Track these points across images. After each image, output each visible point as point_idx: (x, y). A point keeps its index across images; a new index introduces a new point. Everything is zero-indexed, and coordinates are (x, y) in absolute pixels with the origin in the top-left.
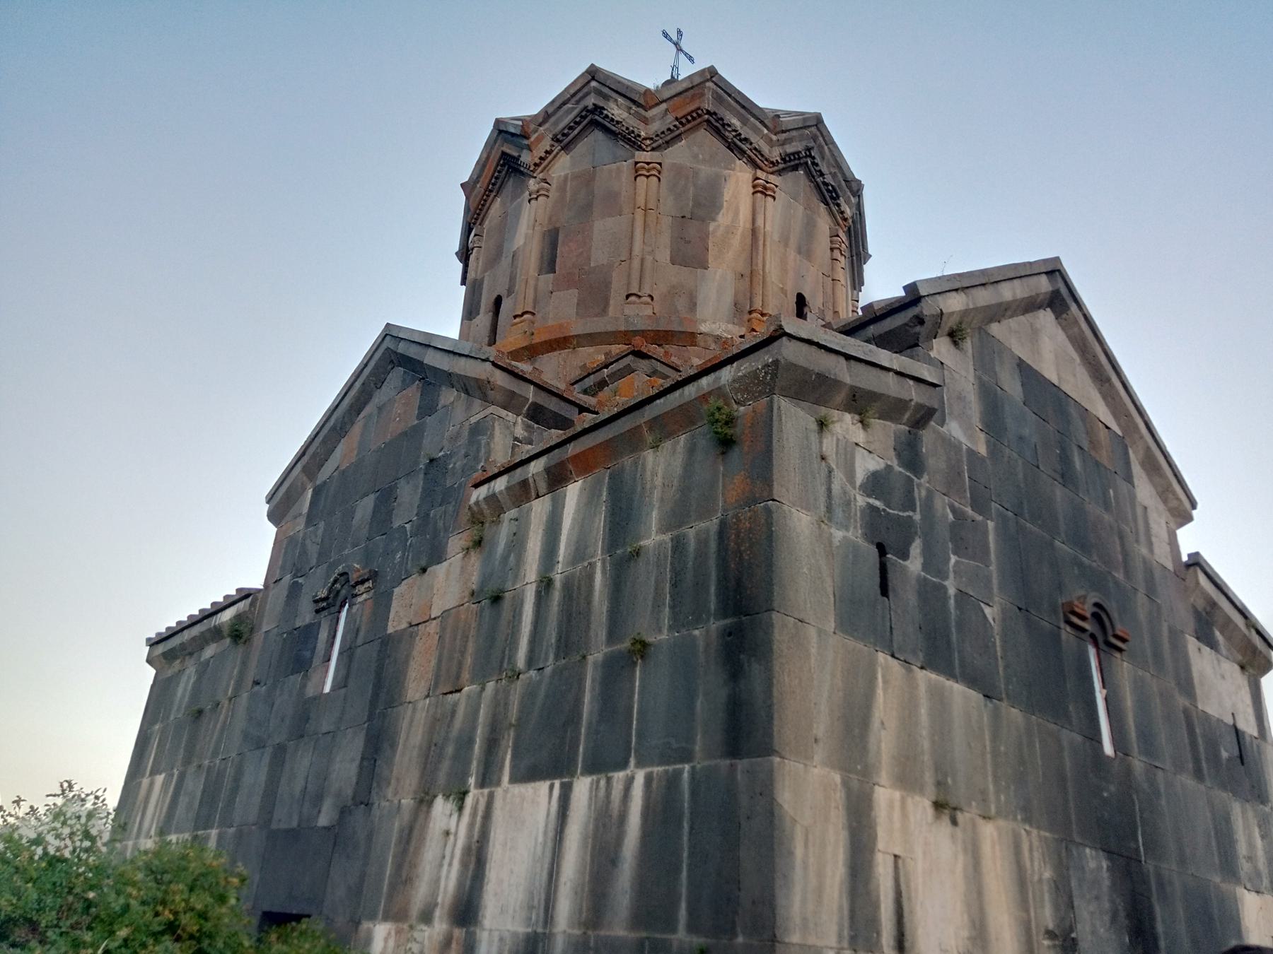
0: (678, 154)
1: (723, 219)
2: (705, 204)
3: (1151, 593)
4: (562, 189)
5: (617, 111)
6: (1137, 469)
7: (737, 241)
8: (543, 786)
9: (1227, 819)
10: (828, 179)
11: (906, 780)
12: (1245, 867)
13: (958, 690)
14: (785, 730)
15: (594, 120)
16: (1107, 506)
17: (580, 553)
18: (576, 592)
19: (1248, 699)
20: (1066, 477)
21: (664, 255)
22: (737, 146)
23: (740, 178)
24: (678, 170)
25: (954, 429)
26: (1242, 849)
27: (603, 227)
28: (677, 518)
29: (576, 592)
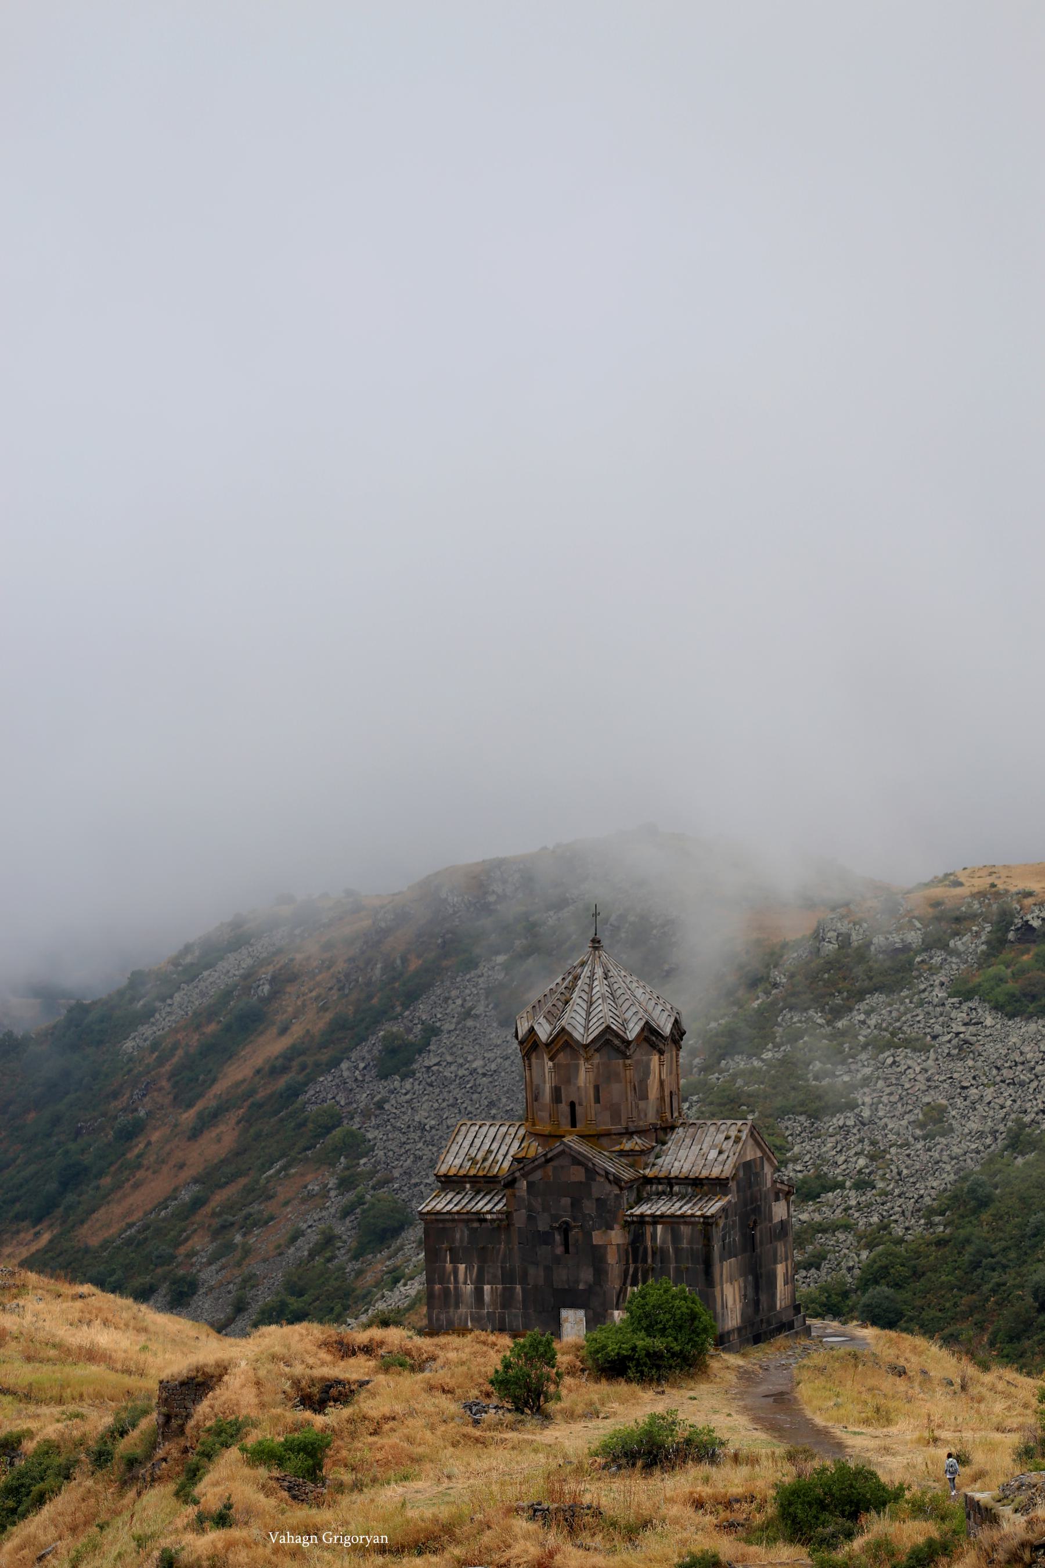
0: (637, 1056)
1: (651, 1077)
2: (647, 1073)
3: (765, 1198)
4: (598, 1067)
5: (616, 1042)
6: (765, 1162)
12: (779, 1258)
15: (608, 1042)
17: (664, 1241)
20: (750, 1187)
22: (653, 1046)
23: (655, 1058)
27: (616, 1088)
28: (690, 1242)
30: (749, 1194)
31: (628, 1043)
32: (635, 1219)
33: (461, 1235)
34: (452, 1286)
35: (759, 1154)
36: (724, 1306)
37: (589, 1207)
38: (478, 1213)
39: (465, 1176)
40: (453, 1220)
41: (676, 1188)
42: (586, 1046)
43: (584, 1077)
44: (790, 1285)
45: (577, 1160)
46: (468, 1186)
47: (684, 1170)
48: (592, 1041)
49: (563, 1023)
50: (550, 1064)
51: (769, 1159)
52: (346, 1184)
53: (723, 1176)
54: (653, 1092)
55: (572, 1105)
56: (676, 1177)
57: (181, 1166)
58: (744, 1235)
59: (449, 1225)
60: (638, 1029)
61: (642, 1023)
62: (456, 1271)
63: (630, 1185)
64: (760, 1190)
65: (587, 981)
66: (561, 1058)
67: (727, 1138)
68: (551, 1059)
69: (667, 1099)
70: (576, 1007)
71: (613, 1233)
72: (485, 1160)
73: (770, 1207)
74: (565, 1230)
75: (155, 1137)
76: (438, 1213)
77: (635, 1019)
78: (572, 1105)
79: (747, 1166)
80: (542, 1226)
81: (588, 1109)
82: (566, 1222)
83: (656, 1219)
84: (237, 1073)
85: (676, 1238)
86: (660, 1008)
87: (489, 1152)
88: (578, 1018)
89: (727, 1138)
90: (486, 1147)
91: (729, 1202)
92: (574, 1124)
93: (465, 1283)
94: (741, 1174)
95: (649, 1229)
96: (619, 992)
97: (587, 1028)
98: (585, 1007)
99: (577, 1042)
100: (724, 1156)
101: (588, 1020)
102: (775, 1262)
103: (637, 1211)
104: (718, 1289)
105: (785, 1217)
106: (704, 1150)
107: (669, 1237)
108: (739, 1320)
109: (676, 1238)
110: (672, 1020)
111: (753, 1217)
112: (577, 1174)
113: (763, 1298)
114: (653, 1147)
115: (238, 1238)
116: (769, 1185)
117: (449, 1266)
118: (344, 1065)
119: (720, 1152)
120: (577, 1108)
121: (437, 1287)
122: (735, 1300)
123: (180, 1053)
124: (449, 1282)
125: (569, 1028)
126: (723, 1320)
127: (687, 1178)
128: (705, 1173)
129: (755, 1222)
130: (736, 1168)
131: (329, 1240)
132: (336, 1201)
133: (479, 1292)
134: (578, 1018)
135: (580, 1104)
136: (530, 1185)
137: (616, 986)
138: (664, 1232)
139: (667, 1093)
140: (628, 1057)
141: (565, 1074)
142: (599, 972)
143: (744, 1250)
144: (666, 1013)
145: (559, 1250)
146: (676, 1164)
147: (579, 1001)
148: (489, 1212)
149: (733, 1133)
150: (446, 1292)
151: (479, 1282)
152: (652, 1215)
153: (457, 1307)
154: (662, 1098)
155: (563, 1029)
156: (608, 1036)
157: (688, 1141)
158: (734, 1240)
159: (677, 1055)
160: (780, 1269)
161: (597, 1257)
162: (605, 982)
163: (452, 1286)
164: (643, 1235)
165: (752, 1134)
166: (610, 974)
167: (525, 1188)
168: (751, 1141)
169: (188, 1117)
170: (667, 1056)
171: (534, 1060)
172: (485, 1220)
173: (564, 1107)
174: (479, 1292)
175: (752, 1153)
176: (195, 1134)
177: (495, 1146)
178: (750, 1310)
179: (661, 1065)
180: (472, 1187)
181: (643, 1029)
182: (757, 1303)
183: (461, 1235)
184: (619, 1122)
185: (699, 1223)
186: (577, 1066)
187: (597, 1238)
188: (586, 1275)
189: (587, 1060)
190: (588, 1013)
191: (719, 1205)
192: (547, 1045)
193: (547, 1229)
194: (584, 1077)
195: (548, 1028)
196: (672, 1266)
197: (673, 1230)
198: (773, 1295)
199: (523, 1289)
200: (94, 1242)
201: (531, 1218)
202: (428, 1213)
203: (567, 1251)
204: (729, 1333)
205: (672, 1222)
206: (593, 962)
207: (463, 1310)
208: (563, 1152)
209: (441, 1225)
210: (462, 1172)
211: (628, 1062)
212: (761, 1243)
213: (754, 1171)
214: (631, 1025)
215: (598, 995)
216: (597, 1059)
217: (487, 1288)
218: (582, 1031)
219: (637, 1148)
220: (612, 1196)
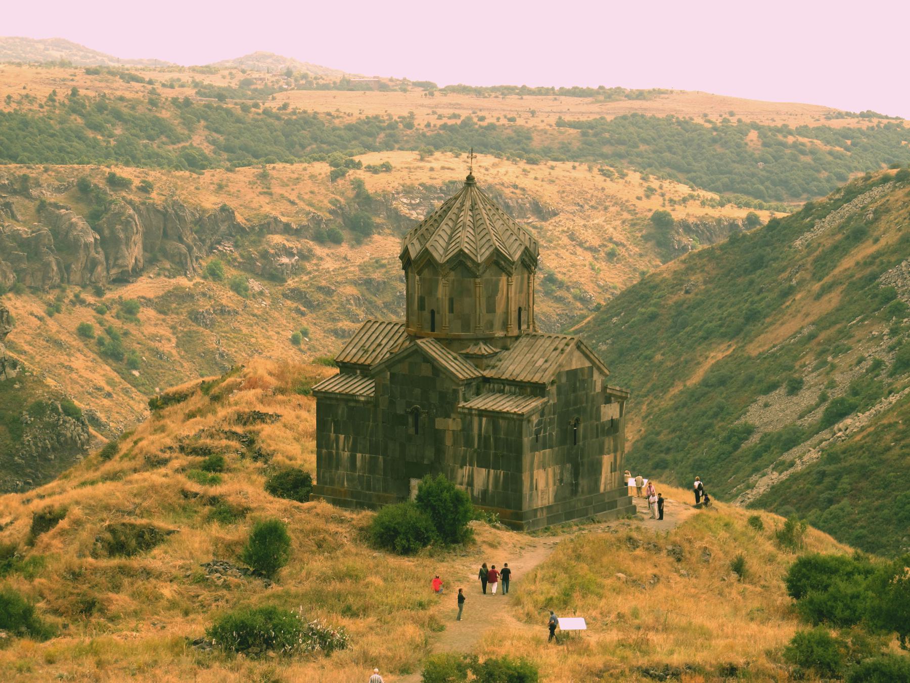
0: (487, 276)
1: (499, 295)
2: (493, 291)
3: (593, 401)
5: (469, 264)
7: (503, 302)
8: (484, 470)
9: (603, 443)
10: (528, 262)
11: (538, 469)
12: (606, 450)
13: (547, 451)
14: (524, 470)
15: (461, 263)
16: (584, 389)
17: (487, 431)
18: (487, 439)
19: (618, 410)
20: (574, 390)
21: (484, 311)
22: (503, 269)
23: (504, 278)
26: (606, 446)
29: (487, 439)
30: (572, 396)
31: (478, 265)
32: (466, 411)
33: (342, 410)
34: (334, 451)
35: (588, 364)
36: (533, 487)
37: (434, 398)
38: (353, 395)
39: (355, 364)
40: (337, 399)
41: (507, 388)
42: (442, 265)
43: (442, 291)
44: (617, 474)
45: (428, 359)
46: (358, 372)
47: (514, 374)
48: (447, 261)
49: (428, 245)
50: (417, 277)
51: (599, 369)
52: (894, 332)
54: (500, 309)
55: (433, 313)
56: (506, 379)
57: (807, 315)
59: (334, 402)
60: (488, 253)
61: (491, 249)
63: (468, 383)
64: (587, 394)
65: (456, 211)
66: (426, 273)
67: (556, 349)
68: (419, 273)
69: (514, 316)
70: (441, 233)
71: (450, 421)
72: (374, 351)
73: (598, 409)
74: (416, 414)
75: (798, 297)
76: (326, 392)
77: (486, 246)
78: (433, 313)
79: (573, 374)
80: (400, 411)
81: (444, 316)
82: (416, 409)
83: (482, 413)
84: (847, 263)
85: (496, 429)
86: (514, 237)
87: (379, 345)
88: (441, 241)
89: (556, 349)
90: (378, 342)
91: (546, 403)
92: (433, 330)
93: (344, 450)
94: (564, 380)
95: (476, 420)
96: (480, 222)
97: (446, 250)
98: (449, 232)
99: (435, 261)
101: (448, 244)
102: (601, 452)
103: (468, 405)
105: (616, 416)
106: (536, 357)
107: (491, 428)
108: (551, 499)
109: (496, 429)
110: (523, 248)
111: (576, 416)
112: (426, 370)
113: (584, 483)
114: (496, 353)
115: (830, 359)
116: (598, 389)
117: (333, 435)
118: (903, 264)
120: (436, 315)
121: (324, 451)
122: (547, 484)
123: (820, 249)
124: (332, 448)
125: (430, 249)
127: (514, 380)
128: (528, 379)
129: (577, 420)
131: (878, 365)
132: (886, 342)
133: (353, 459)
134: (441, 241)
135: (438, 313)
136: (393, 376)
137: (478, 217)
138: (488, 423)
140: (477, 277)
141: (430, 288)
142: (468, 204)
144: (518, 242)
145: (412, 431)
147: (445, 227)
148: (361, 395)
149: (561, 347)
150: (330, 454)
151: (354, 450)
152: (478, 409)
153: (337, 468)
154: (507, 313)
155: (427, 249)
156: (461, 258)
157: (526, 349)
158: (551, 434)
159: (529, 278)
161: (437, 438)
162: (470, 213)
163: (334, 451)
164: (471, 422)
166: (477, 207)
167: (388, 377)
168: (577, 354)
169: (816, 287)
170: (515, 279)
171: (410, 274)
172: (358, 401)
173: (427, 314)
174: (353, 459)
175: (577, 362)
176: (818, 297)
177: (384, 342)
179: (509, 284)
180: (361, 373)
181: (491, 255)
183: (342, 410)
184: (468, 331)
185: (513, 419)
186: (437, 281)
187: (440, 423)
188: (430, 453)
189: (445, 276)
190: (451, 238)
191: (534, 404)
192: (416, 261)
193: (402, 412)
194: (442, 291)
196: (492, 452)
197: (494, 422)
198: (597, 482)
199: (385, 461)
200: (754, 353)
201: (392, 403)
202: (319, 391)
203: (417, 432)
204: (536, 511)
205: (494, 416)
206: (465, 196)
207: (341, 472)
208: (416, 350)
209: (328, 402)
210: (355, 360)
211: (478, 280)
213: (581, 377)
214: (483, 250)
215: (461, 224)
216: (452, 276)
217: (359, 455)
218: (441, 252)
219: (479, 353)
220: (451, 391)
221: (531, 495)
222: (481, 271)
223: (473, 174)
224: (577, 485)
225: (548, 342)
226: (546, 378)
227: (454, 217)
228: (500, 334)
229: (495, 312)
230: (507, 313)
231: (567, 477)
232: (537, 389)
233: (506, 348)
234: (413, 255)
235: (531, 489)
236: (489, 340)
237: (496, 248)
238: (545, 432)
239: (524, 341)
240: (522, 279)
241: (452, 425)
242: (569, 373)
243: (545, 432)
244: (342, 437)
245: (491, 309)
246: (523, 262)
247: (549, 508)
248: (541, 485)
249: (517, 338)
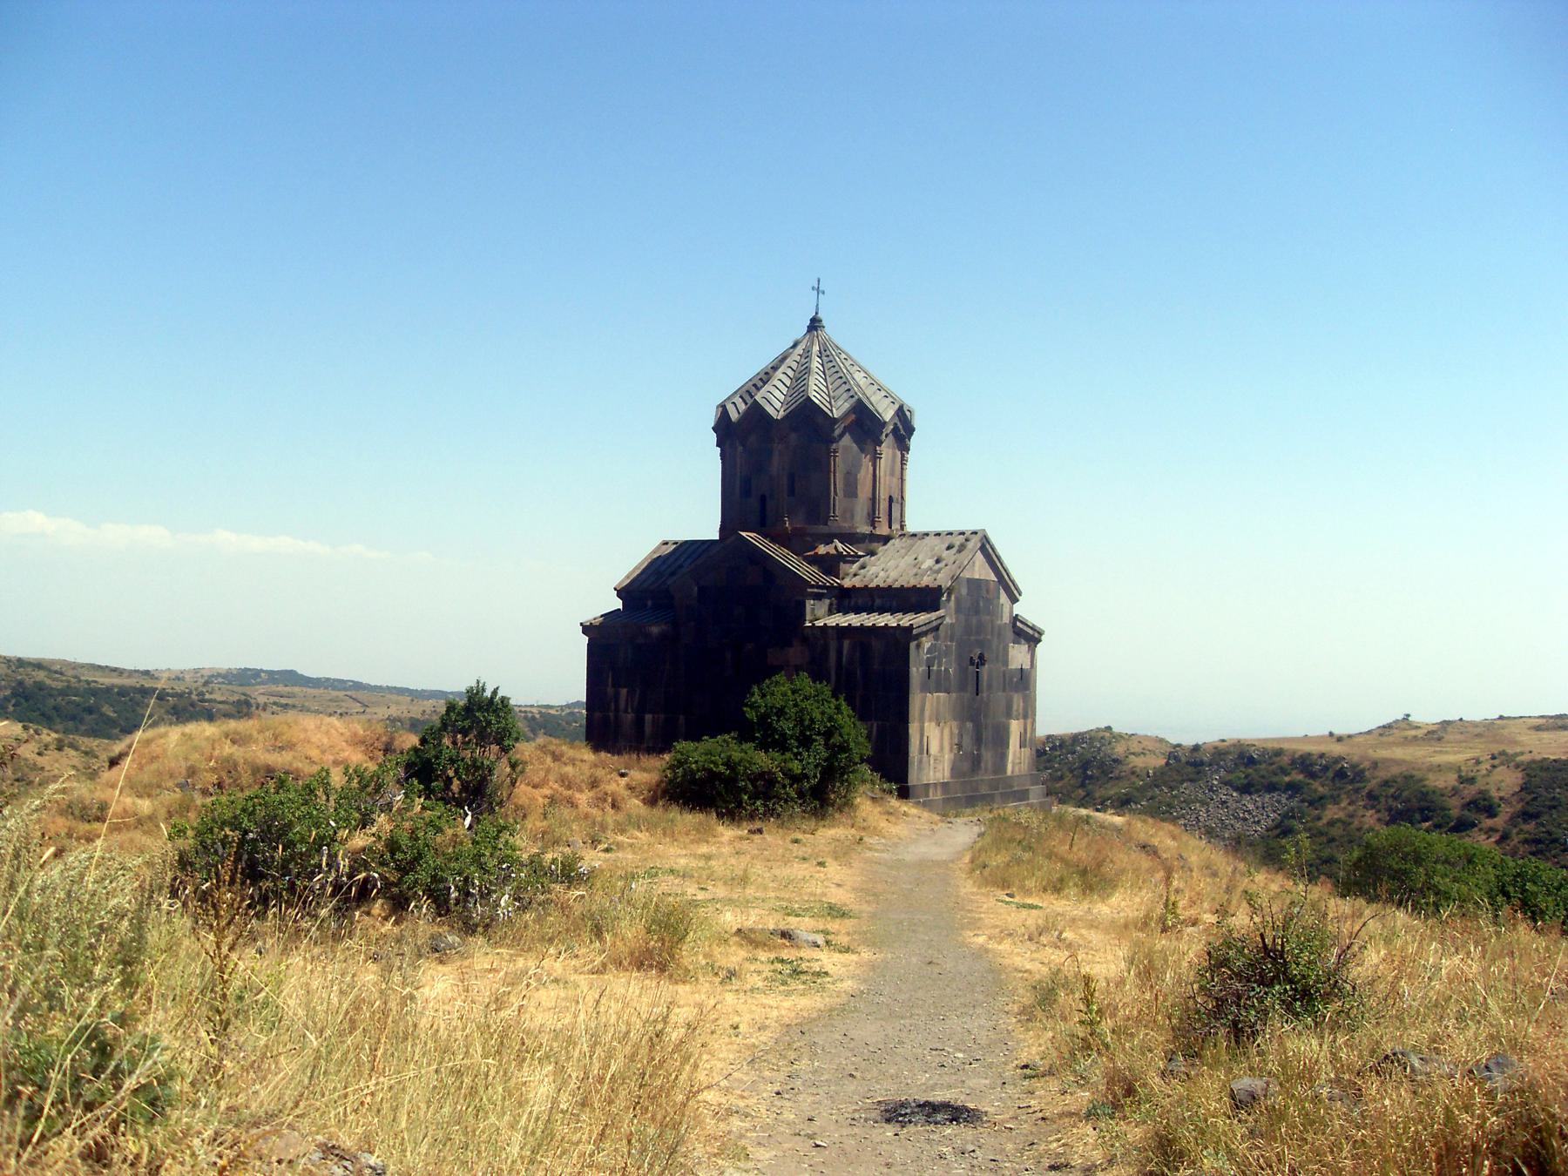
1: (863, 472)
5: (820, 420)
20: (977, 612)
24: (846, 448)
25: (948, 620)
30: (974, 620)
31: (835, 421)
35: (993, 577)
41: (878, 602)
46: (649, 603)
50: (740, 448)
53: (934, 585)
54: (864, 492)
55: (763, 499)
58: (962, 671)
60: (847, 406)
62: (617, 696)
67: (949, 548)
69: (883, 506)
78: (763, 499)
79: (975, 585)
89: (949, 548)
93: (626, 711)
94: (964, 591)
95: (833, 645)
100: (941, 565)
102: (1009, 715)
104: (913, 729)
105: (1027, 666)
108: (947, 773)
113: (988, 756)
116: (1006, 619)
117: (610, 690)
119: (938, 561)
121: (597, 714)
122: (942, 748)
126: (920, 769)
128: (913, 582)
130: (956, 579)
133: (639, 722)
136: (702, 590)
139: (883, 496)
142: (816, 348)
143: (962, 687)
146: (882, 574)
160: (1015, 727)
164: (826, 649)
165: (983, 549)
168: (979, 555)
174: (639, 722)
178: (966, 766)
182: (976, 762)
194: (778, 464)
195: (742, 407)
212: (990, 687)
217: (648, 717)
218: (778, 405)
221: (920, 761)
222: (837, 432)
223: (820, 315)
224: (979, 756)
225: (937, 540)
226: (943, 580)
227: (794, 366)
228: (865, 529)
229: (856, 496)
230: (874, 500)
231: (967, 741)
232: (925, 598)
233: (872, 553)
234: (734, 416)
235: (921, 752)
236: (850, 538)
237: (860, 400)
238: (940, 665)
239: (895, 543)
240: (894, 456)
241: (795, 653)
242: (969, 581)
243: (940, 665)
244: (624, 691)
245: (851, 491)
246: (895, 431)
247: (945, 785)
248: (934, 749)
249: (886, 540)
